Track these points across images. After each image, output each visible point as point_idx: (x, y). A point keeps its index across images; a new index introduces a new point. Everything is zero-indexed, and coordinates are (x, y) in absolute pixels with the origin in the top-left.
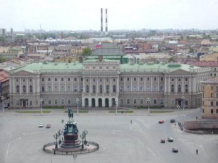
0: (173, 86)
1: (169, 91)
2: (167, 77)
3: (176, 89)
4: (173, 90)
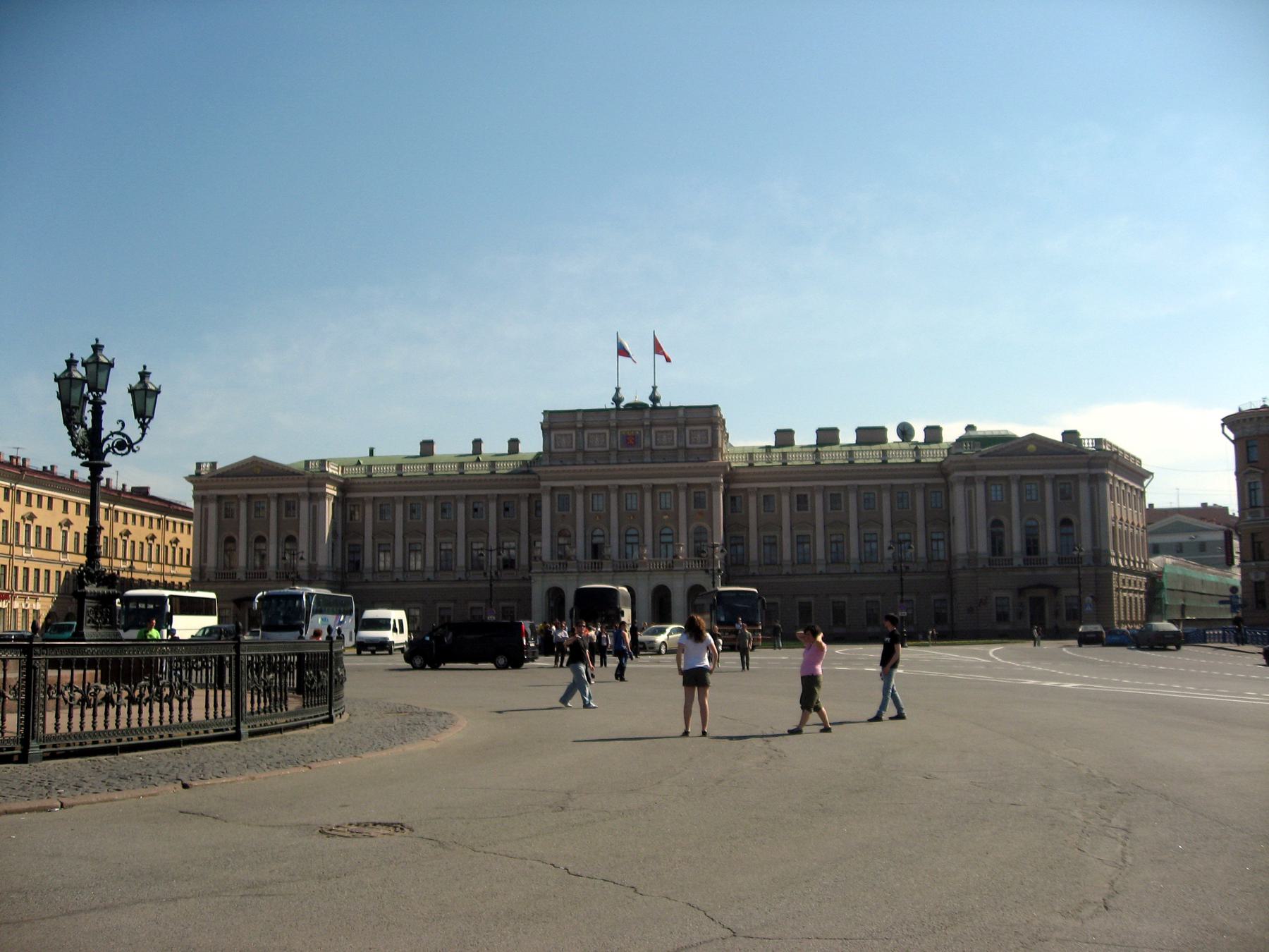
0: (997, 523)
1: (983, 546)
2: (969, 481)
3: (1016, 543)
4: (997, 544)
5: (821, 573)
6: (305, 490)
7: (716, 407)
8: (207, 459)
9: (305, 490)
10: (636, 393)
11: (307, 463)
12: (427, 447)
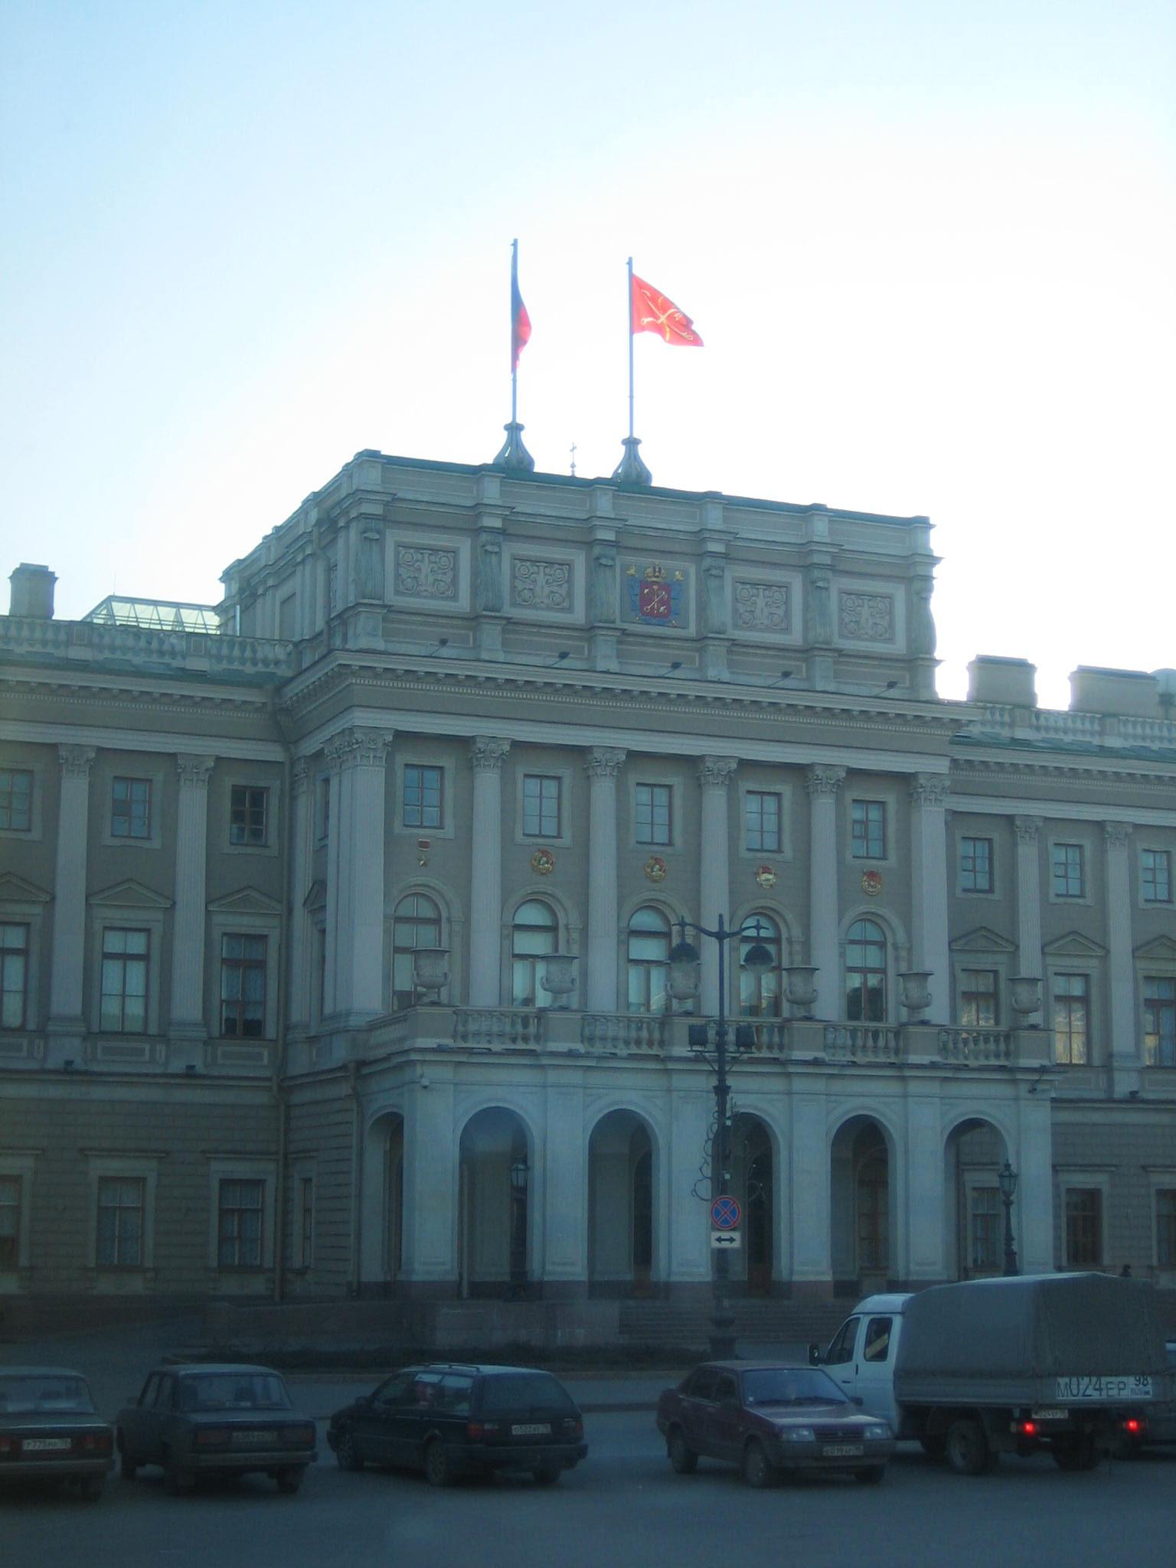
5: (1133, 1098)
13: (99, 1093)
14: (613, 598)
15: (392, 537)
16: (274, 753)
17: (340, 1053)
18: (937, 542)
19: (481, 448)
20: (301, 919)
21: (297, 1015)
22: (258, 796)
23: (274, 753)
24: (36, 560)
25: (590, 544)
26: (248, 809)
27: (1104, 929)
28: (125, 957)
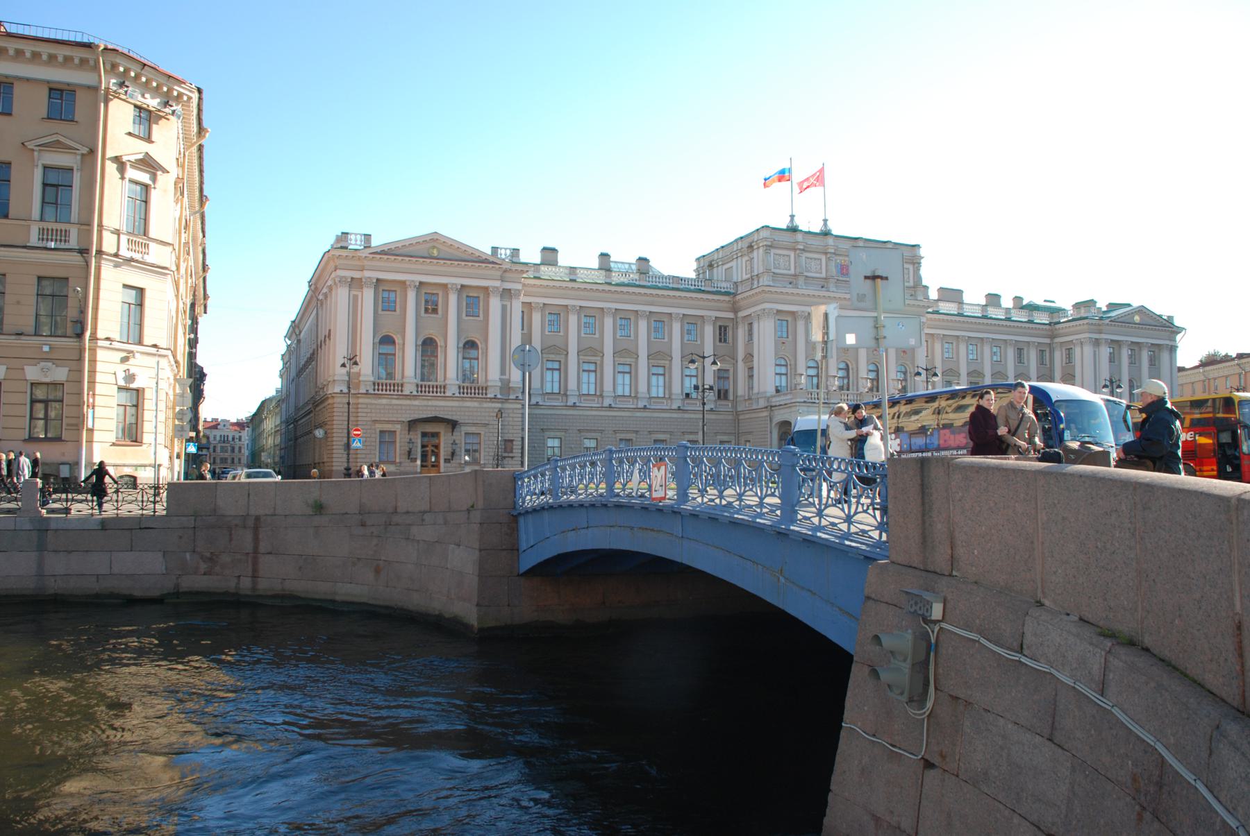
2: (1097, 343)
6: (497, 284)
7: (918, 246)
8: (356, 228)
9: (497, 284)
10: (809, 222)
11: (495, 249)
12: (550, 254)
13: (686, 416)
14: (833, 271)
15: (773, 251)
16: (731, 315)
17: (762, 403)
18: (922, 252)
19: (783, 224)
20: (741, 365)
21: (740, 393)
22: (725, 328)
23: (731, 315)
24: (643, 256)
25: (826, 253)
26: (723, 333)
27: (958, 367)
28: (553, 369)
